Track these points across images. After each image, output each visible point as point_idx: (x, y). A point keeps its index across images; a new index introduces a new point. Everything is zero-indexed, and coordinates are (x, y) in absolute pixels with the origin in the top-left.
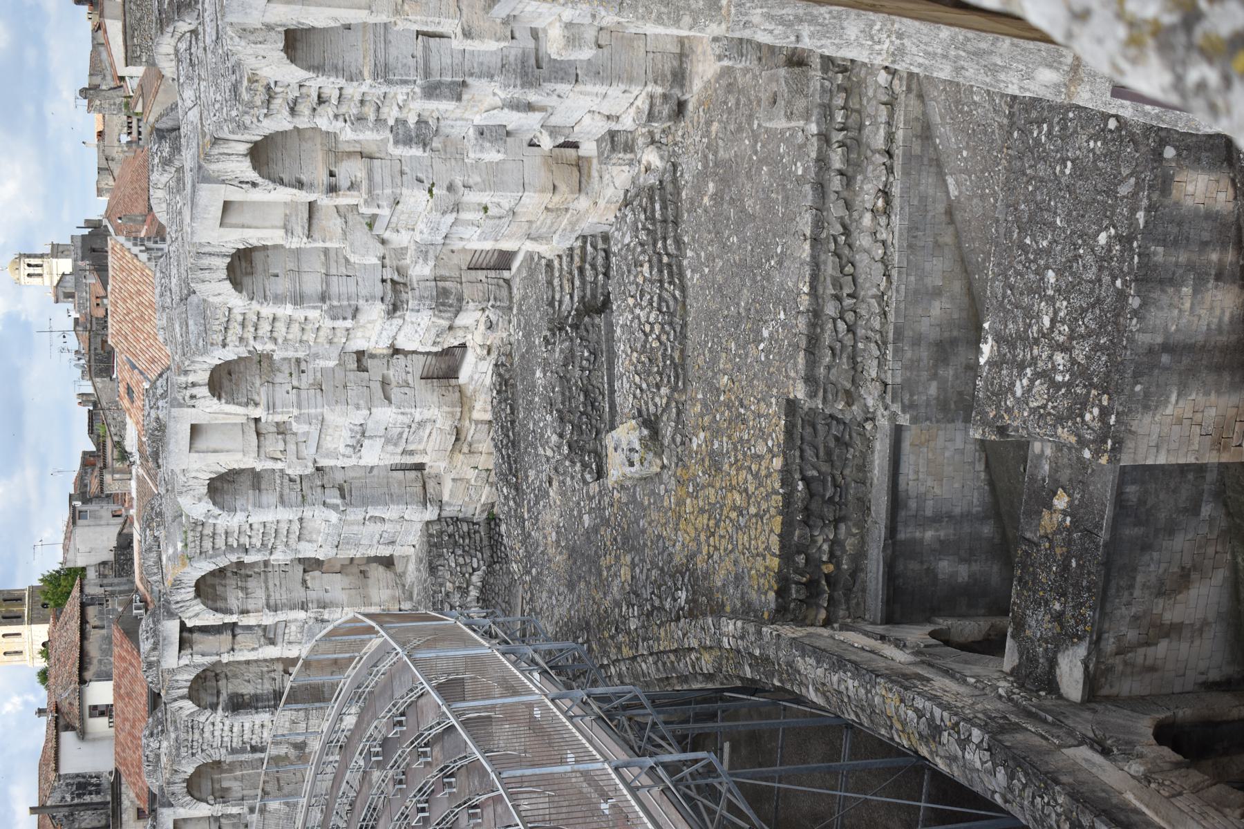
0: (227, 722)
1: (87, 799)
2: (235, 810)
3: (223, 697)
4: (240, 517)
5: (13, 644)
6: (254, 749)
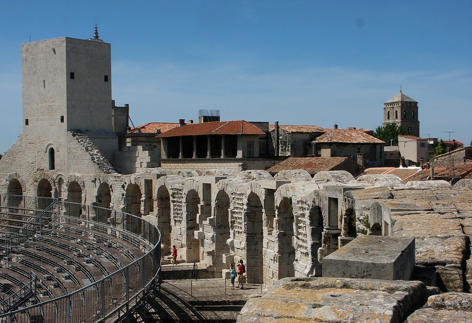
0: (243, 211)
1: (280, 146)
2: (213, 212)
3: (254, 209)
4: (308, 222)
5: (392, 116)
6: (233, 222)
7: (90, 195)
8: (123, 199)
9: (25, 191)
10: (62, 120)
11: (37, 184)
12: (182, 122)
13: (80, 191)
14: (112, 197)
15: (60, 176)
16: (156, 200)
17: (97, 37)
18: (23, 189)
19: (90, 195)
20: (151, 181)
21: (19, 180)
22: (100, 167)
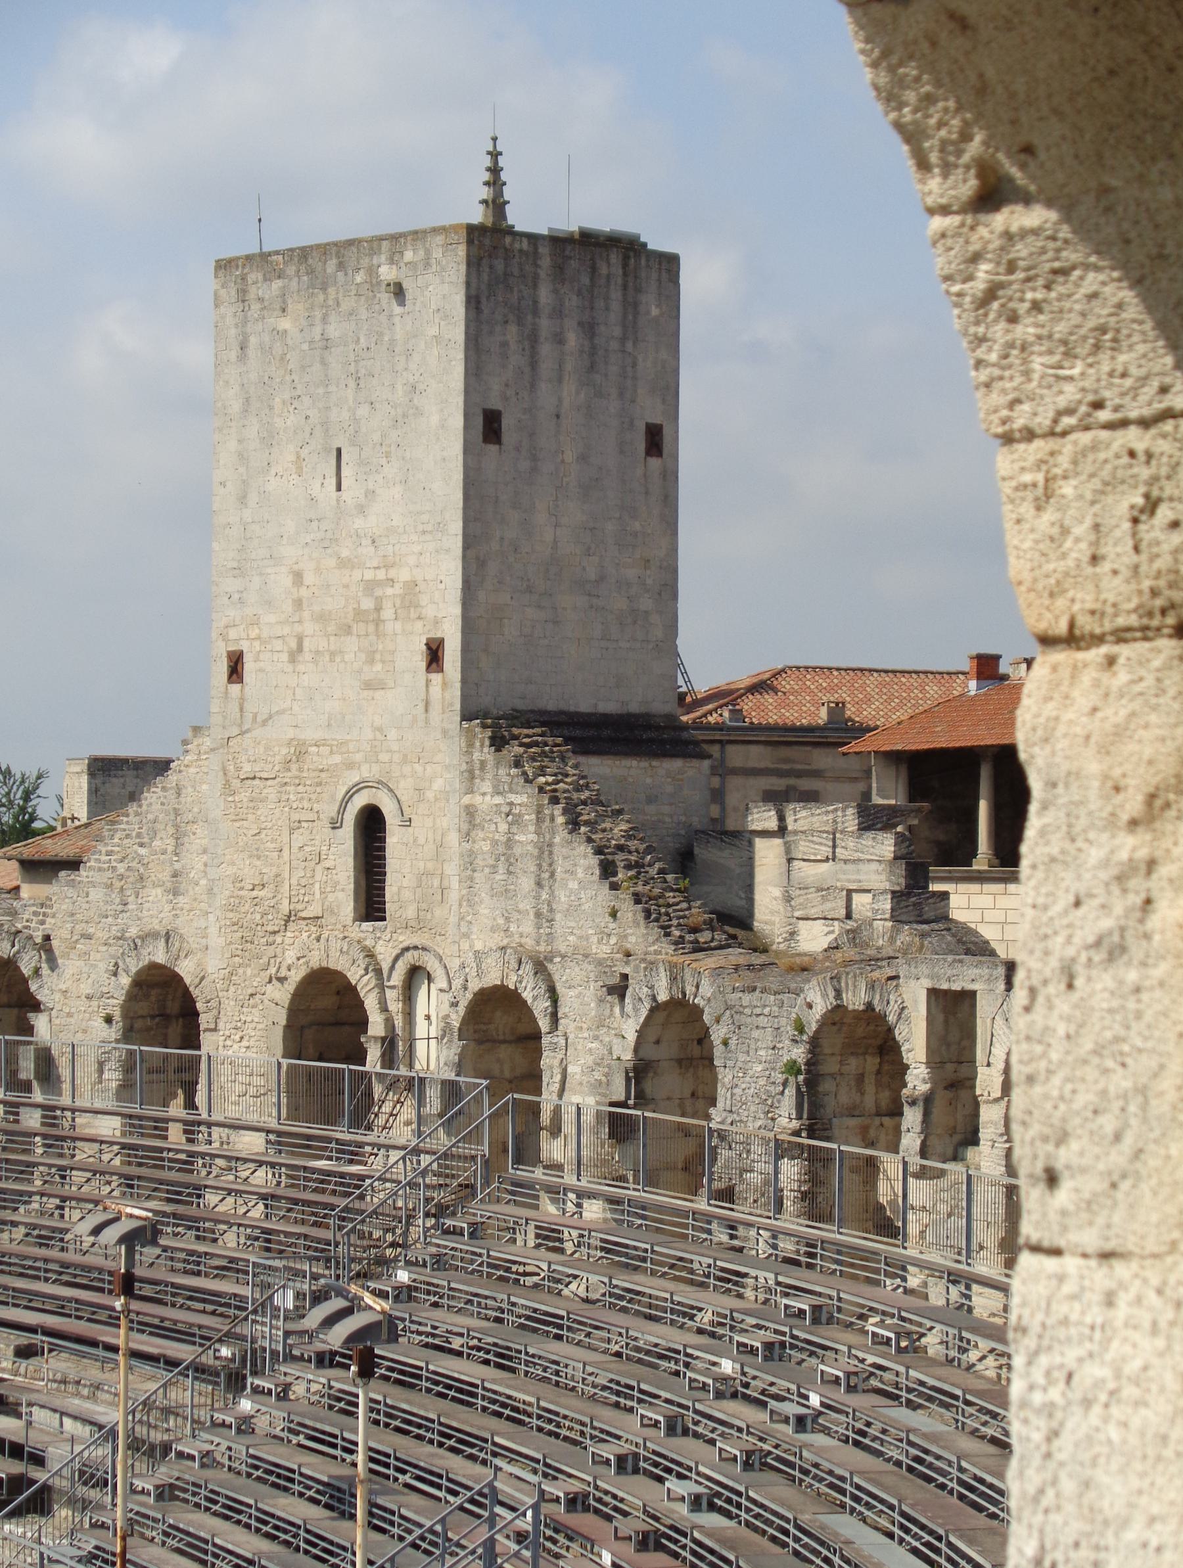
7: (586, 1058)
8: (790, 1092)
9: (215, 1030)
10: (434, 655)
11: (283, 994)
12: (987, 667)
13: (531, 1040)
14: (725, 1077)
15: (410, 957)
16: (996, 1100)
17: (497, 205)
18: (204, 1020)
19: (586, 1058)
20: (969, 997)
21: (186, 970)
22: (648, 914)
